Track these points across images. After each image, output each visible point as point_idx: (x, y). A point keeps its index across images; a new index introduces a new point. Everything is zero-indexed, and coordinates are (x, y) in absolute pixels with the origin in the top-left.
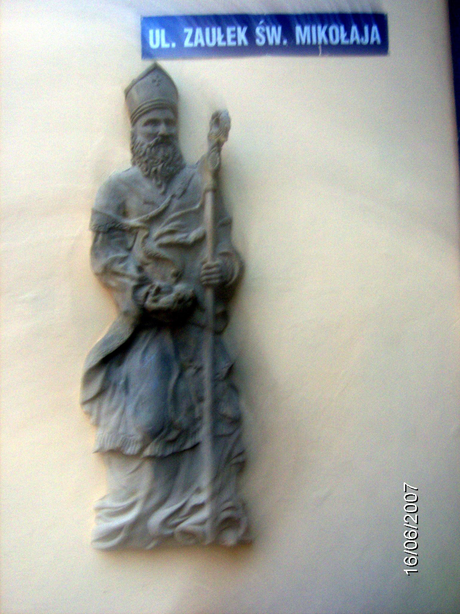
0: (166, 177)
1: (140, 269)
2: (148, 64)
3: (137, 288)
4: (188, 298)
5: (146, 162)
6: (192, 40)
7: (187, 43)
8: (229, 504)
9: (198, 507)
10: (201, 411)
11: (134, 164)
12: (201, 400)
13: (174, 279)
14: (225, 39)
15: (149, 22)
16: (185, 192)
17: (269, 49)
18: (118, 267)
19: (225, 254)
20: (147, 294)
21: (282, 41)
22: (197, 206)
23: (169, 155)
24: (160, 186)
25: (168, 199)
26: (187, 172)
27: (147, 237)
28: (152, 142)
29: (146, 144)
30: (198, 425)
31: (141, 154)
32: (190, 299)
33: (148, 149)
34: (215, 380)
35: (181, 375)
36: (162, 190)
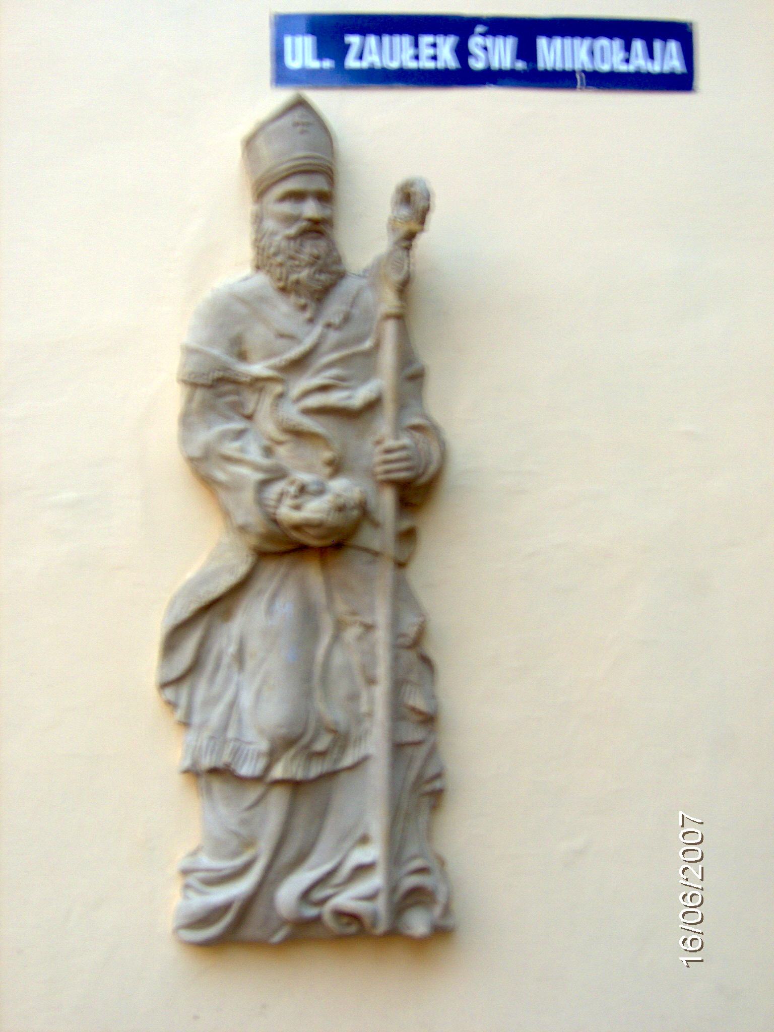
0: (316, 291)
1: (268, 451)
2: (285, 95)
4: (352, 503)
5: (281, 265)
6: (360, 57)
7: (351, 62)
8: (417, 863)
9: (362, 870)
10: (371, 701)
11: (258, 268)
12: (371, 681)
14: (417, 58)
15: (284, 25)
16: (347, 319)
17: (491, 77)
18: (231, 448)
19: (417, 428)
20: (282, 495)
21: (513, 63)
24: (304, 308)
25: (318, 330)
26: (349, 286)
27: (281, 396)
28: (292, 231)
29: (280, 234)
30: (367, 724)
31: (272, 250)
36: (308, 314)
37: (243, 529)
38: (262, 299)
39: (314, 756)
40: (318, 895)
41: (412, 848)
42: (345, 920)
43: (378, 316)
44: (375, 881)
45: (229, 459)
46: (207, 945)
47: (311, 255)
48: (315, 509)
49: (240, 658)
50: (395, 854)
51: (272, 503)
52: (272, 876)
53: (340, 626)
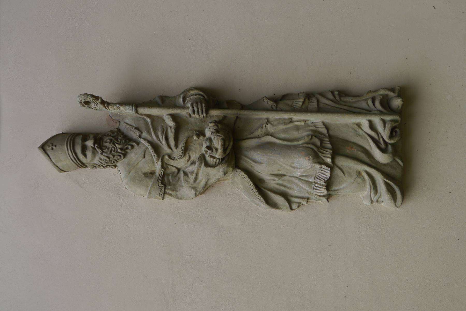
0: (125, 141)
1: (193, 163)
3: (207, 165)
4: (216, 127)
5: (114, 156)
8: (370, 102)
9: (372, 126)
10: (300, 121)
12: (291, 121)
13: (201, 137)
16: (137, 128)
18: (192, 178)
19: (184, 100)
20: (211, 156)
22: (148, 120)
23: (109, 139)
30: (309, 123)
31: (108, 159)
32: (217, 126)
33: (104, 154)
34: (277, 110)
35: (272, 135)
36: (134, 144)
37: (225, 174)
38: (128, 164)
39: (322, 147)
40: (383, 146)
41: (363, 105)
42: (394, 133)
43: (136, 115)
44: (377, 120)
45: (196, 179)
46: (404, 194)
47: (110, 143)
48: (217, 143)
49: (281, 176)
50: (367, 112)
51: (215, 160)
52: (374, 165)
53: (267, 134)
